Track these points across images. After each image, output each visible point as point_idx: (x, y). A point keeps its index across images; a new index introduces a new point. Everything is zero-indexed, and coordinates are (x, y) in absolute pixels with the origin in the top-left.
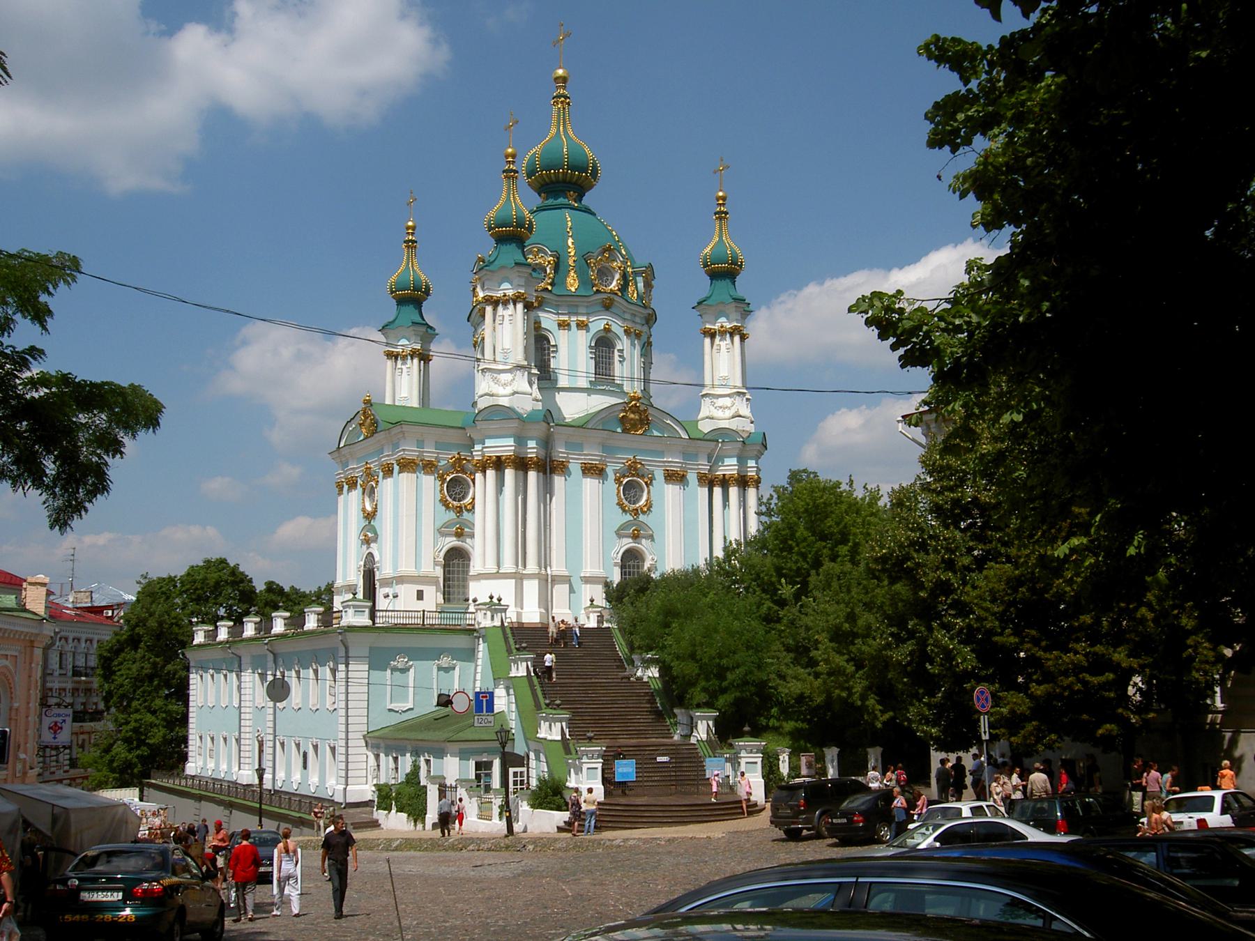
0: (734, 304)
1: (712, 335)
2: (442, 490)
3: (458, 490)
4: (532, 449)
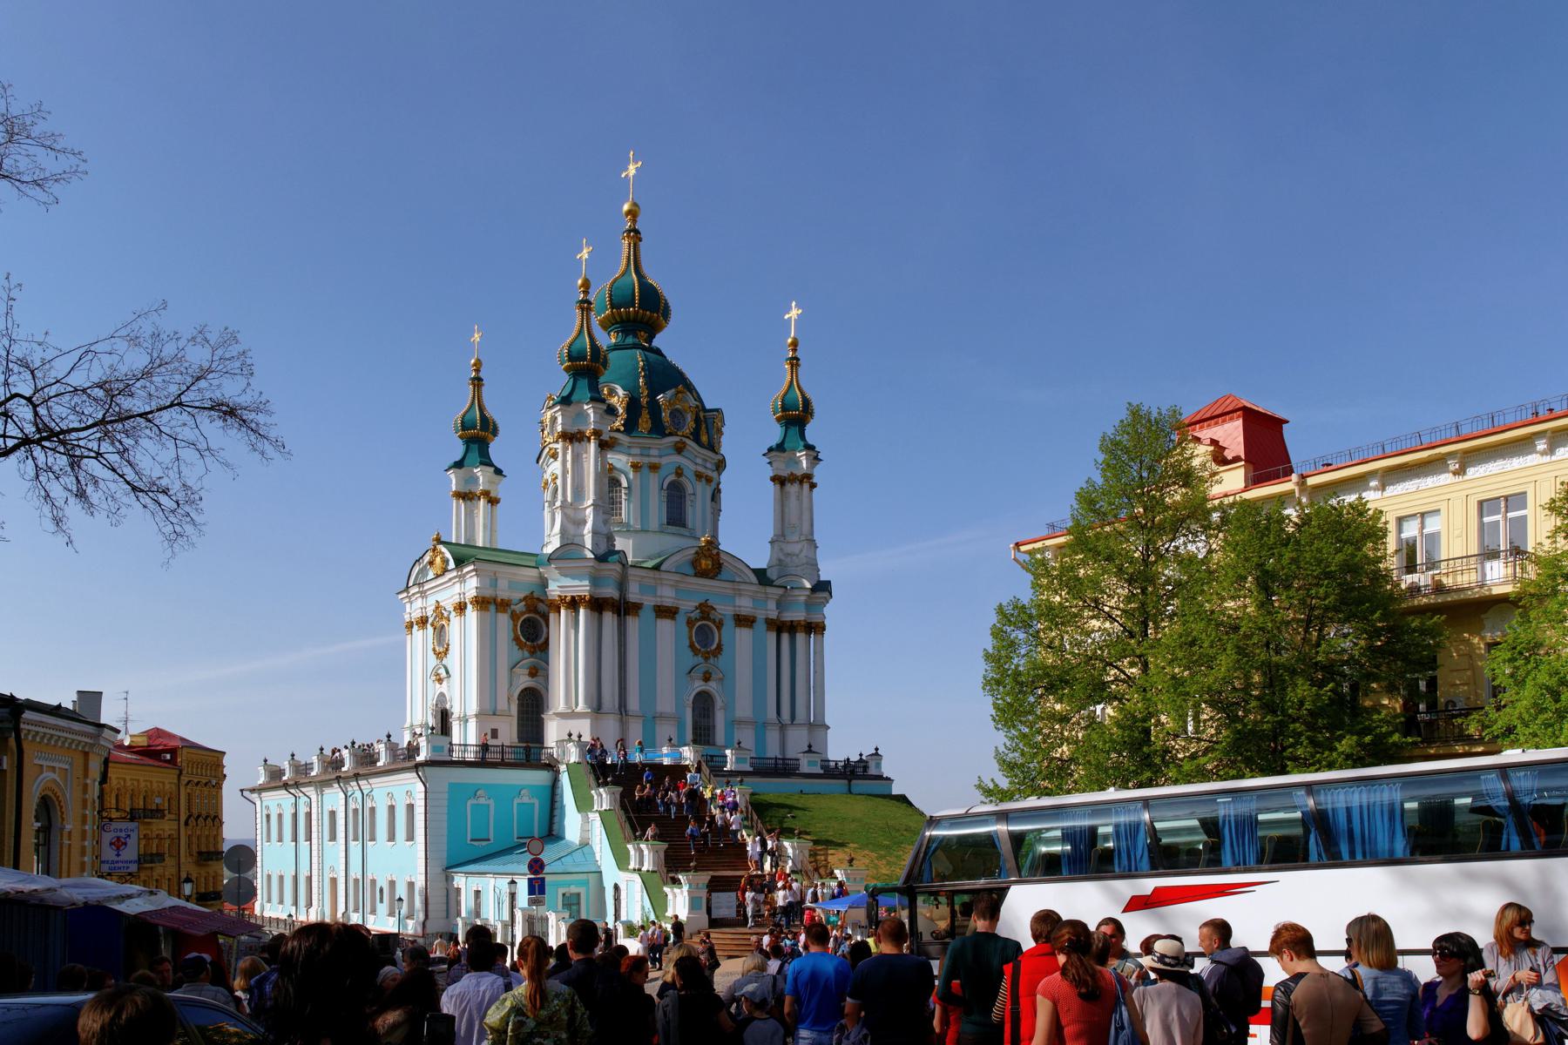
2: (515, 630)
4: (610, 592)
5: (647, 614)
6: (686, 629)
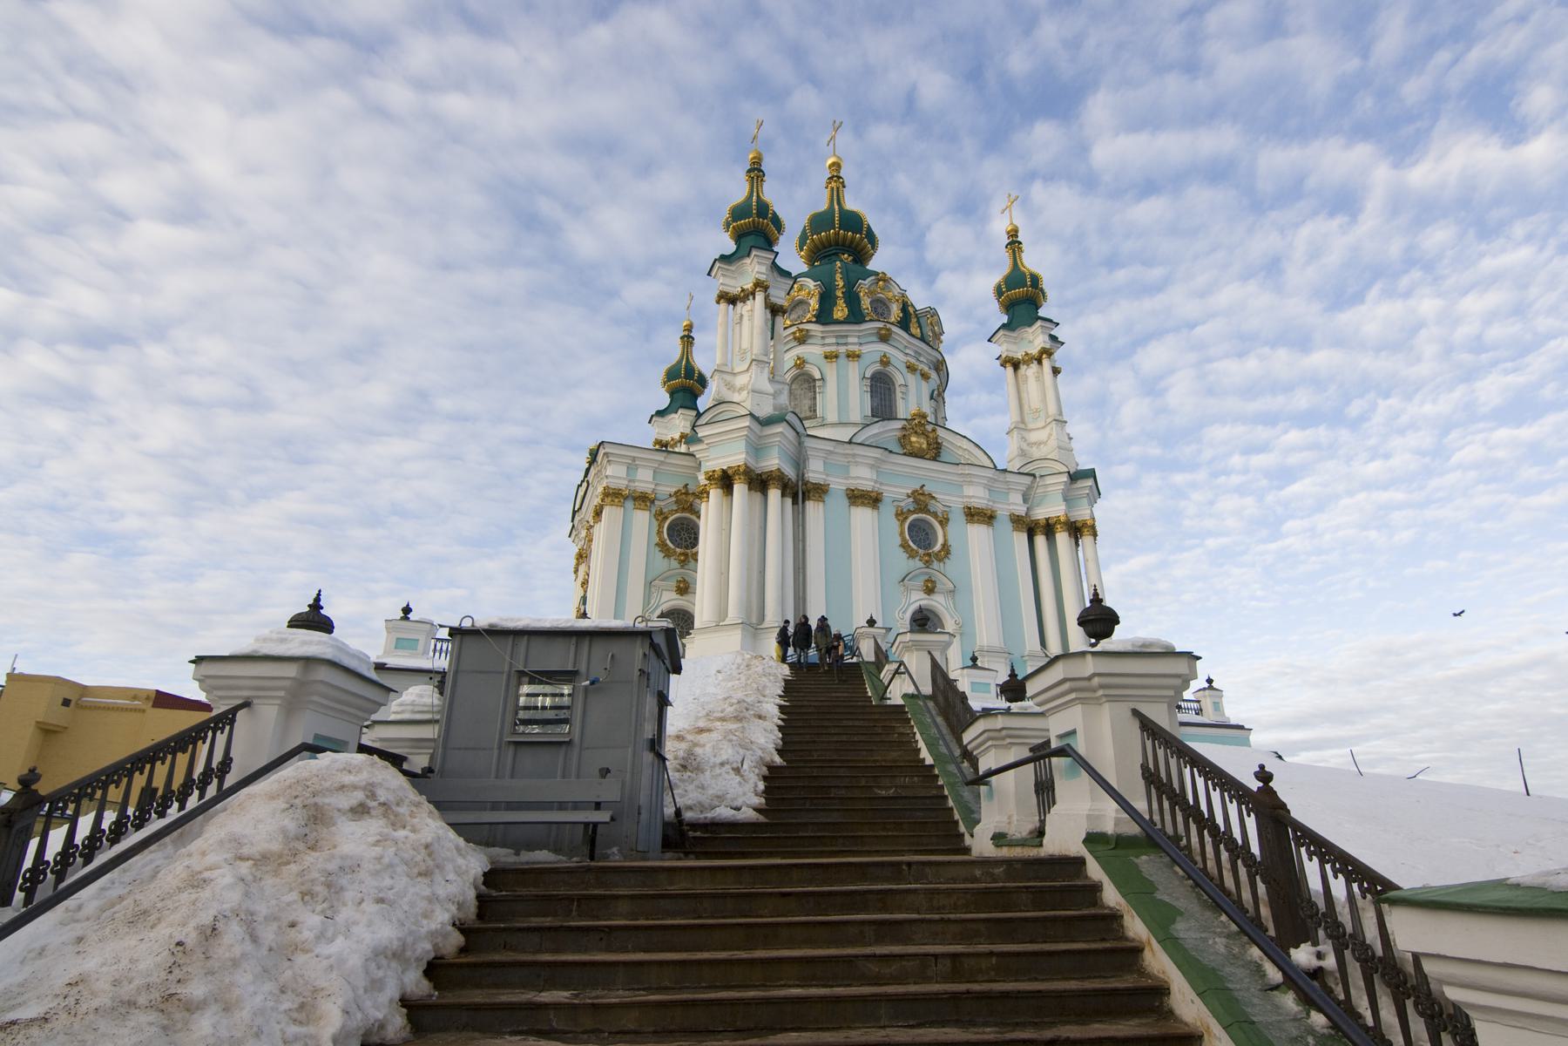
0: (1039, 323)
1: (1016, 365)
2: (660, 533)
3: (685, 535)
4: (773, 461)
5: (837, 500)
6: (894, 524)
